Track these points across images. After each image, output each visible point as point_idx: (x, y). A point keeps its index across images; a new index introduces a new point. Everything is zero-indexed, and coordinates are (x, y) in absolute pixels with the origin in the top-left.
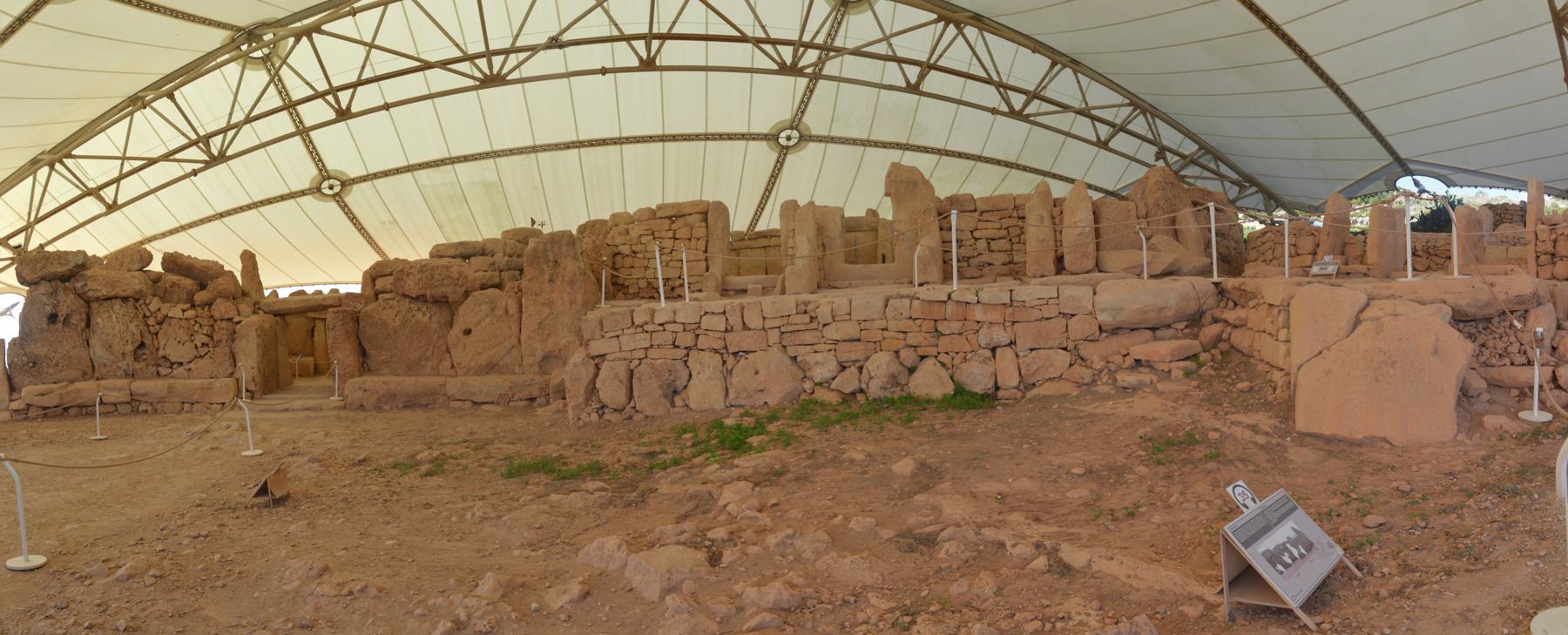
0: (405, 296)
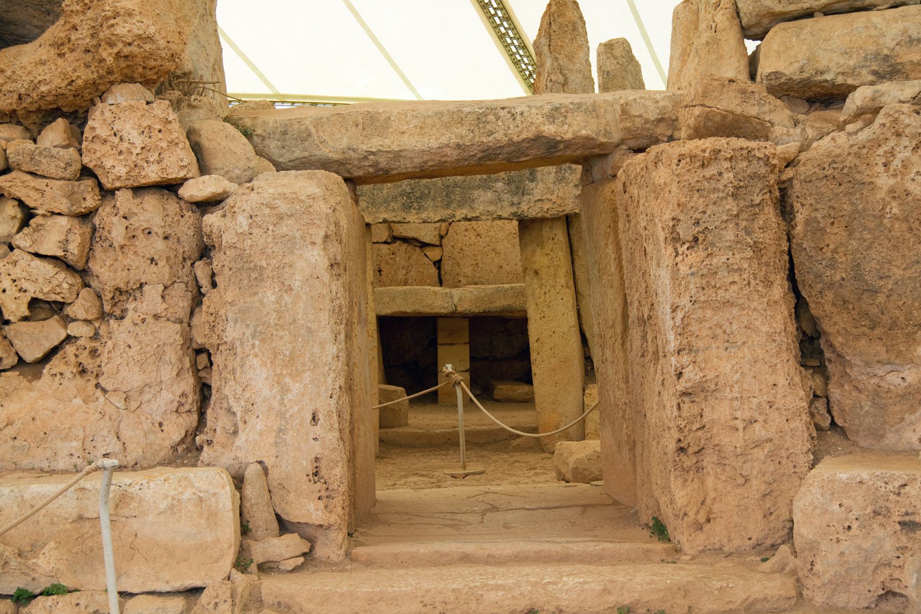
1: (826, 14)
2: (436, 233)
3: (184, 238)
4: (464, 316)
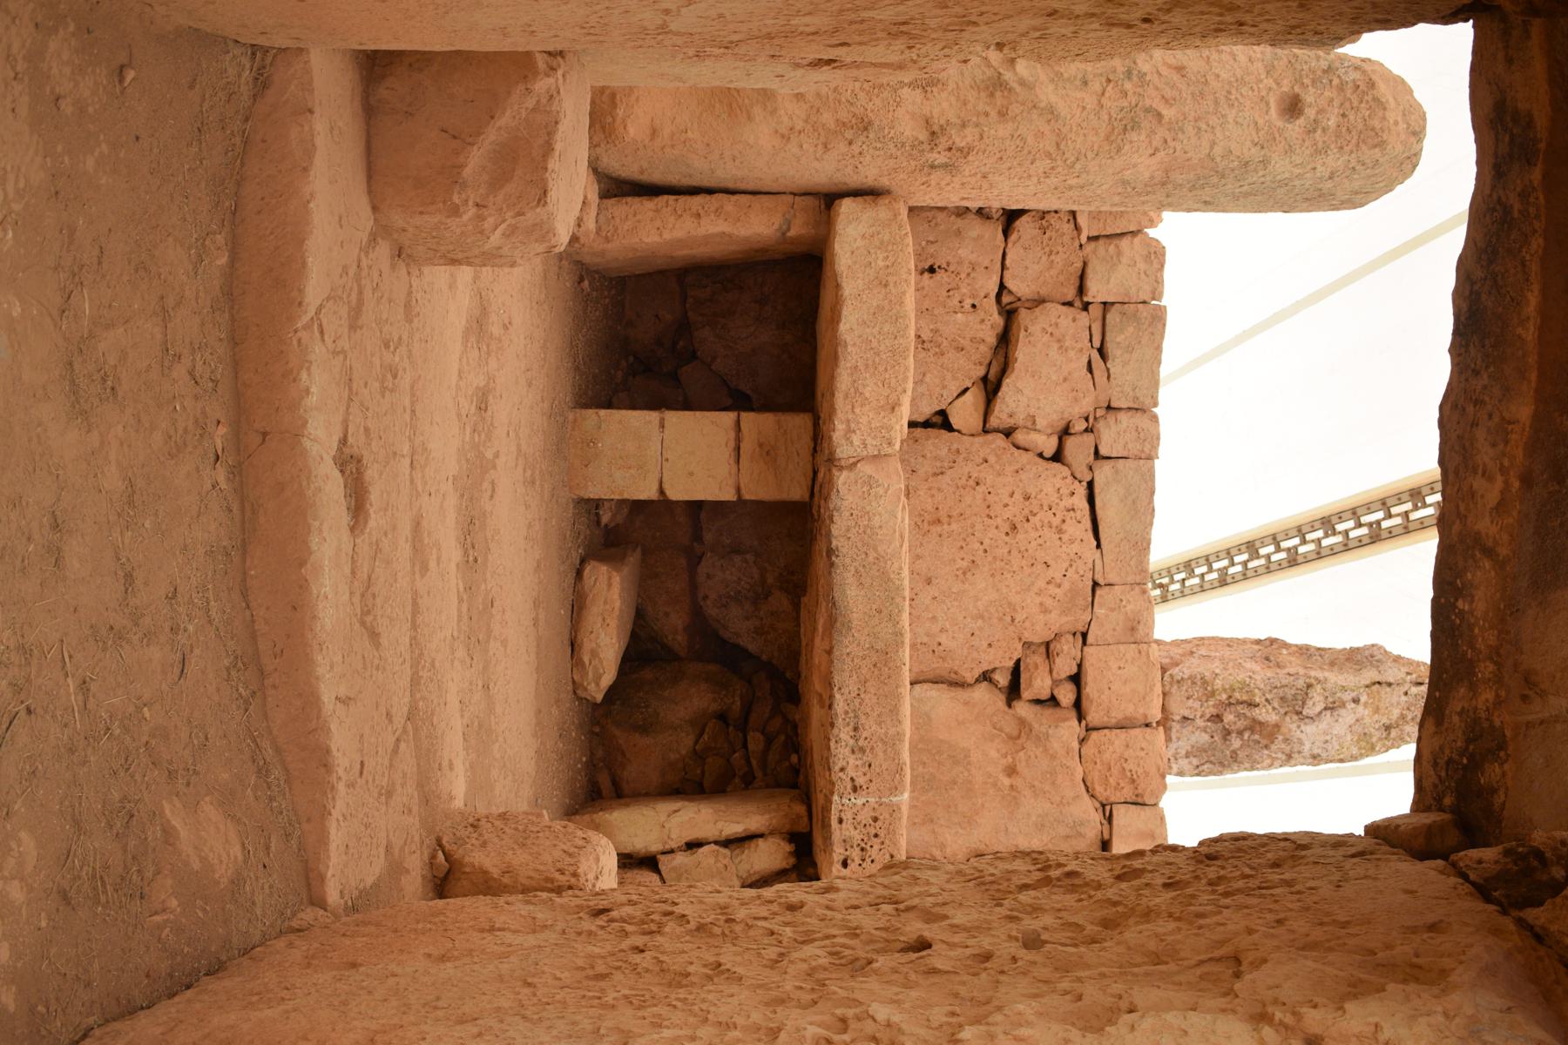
2: (1019, 419)
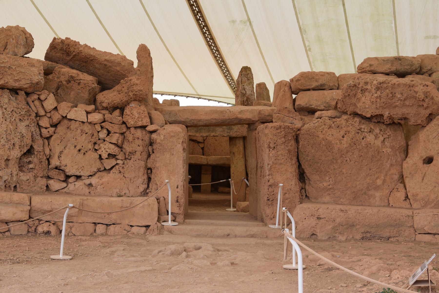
0: (356, 114)
1: (313, 90)
3: (146, 140)
4: (210, 165)
